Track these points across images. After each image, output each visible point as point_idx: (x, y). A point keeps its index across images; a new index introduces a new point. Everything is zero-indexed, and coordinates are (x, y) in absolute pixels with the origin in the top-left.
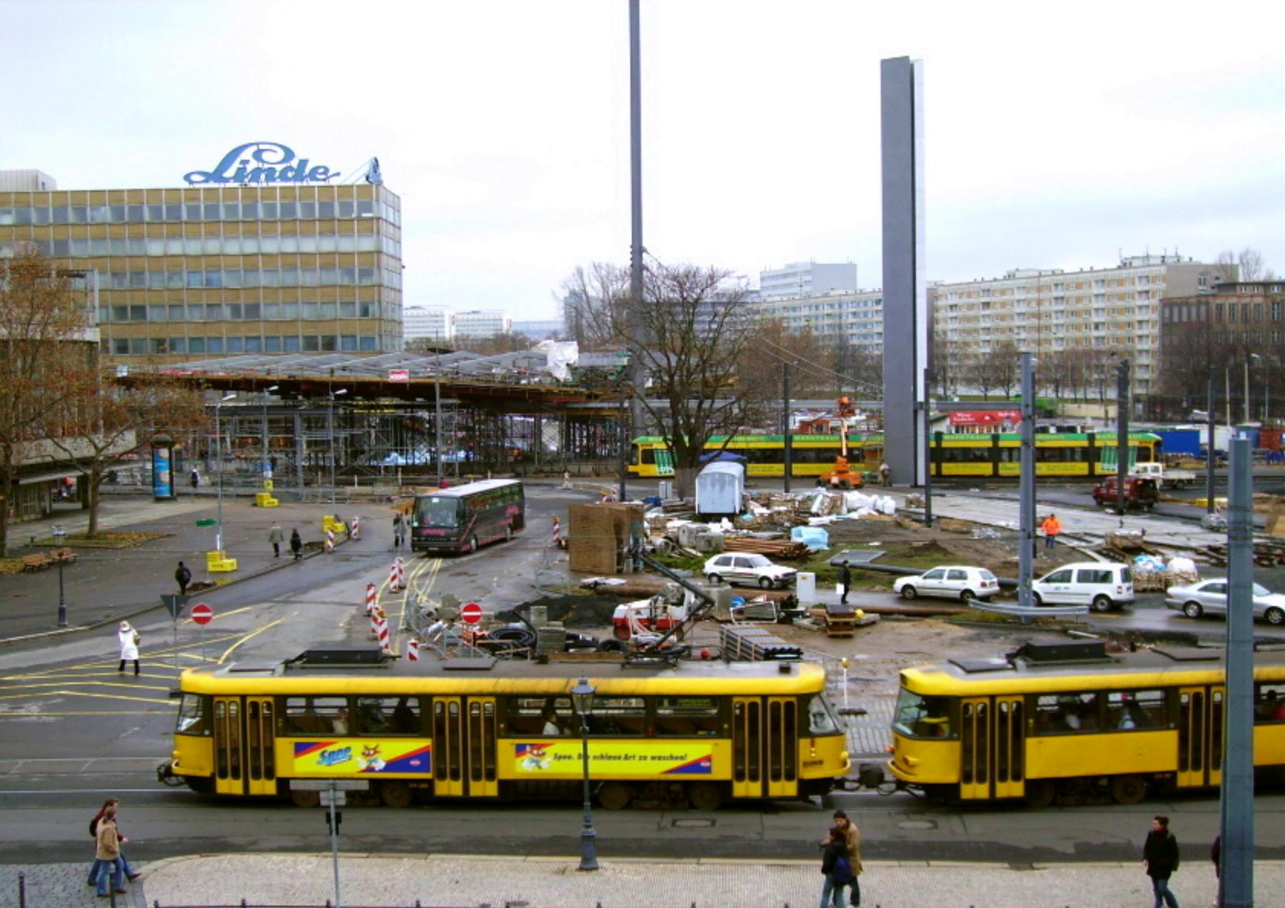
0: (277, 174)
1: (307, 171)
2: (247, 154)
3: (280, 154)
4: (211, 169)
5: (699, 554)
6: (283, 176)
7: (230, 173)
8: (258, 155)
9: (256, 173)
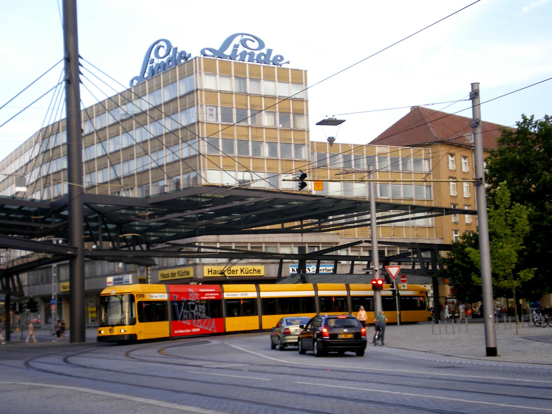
0: (255, 58)
1: (271, 59)
2: (237, 41)
3: (256, 45)
4: (217, 48)
5: (316, 344)
7: (228, 52)
8: (243, 43)
9: (243, 54)
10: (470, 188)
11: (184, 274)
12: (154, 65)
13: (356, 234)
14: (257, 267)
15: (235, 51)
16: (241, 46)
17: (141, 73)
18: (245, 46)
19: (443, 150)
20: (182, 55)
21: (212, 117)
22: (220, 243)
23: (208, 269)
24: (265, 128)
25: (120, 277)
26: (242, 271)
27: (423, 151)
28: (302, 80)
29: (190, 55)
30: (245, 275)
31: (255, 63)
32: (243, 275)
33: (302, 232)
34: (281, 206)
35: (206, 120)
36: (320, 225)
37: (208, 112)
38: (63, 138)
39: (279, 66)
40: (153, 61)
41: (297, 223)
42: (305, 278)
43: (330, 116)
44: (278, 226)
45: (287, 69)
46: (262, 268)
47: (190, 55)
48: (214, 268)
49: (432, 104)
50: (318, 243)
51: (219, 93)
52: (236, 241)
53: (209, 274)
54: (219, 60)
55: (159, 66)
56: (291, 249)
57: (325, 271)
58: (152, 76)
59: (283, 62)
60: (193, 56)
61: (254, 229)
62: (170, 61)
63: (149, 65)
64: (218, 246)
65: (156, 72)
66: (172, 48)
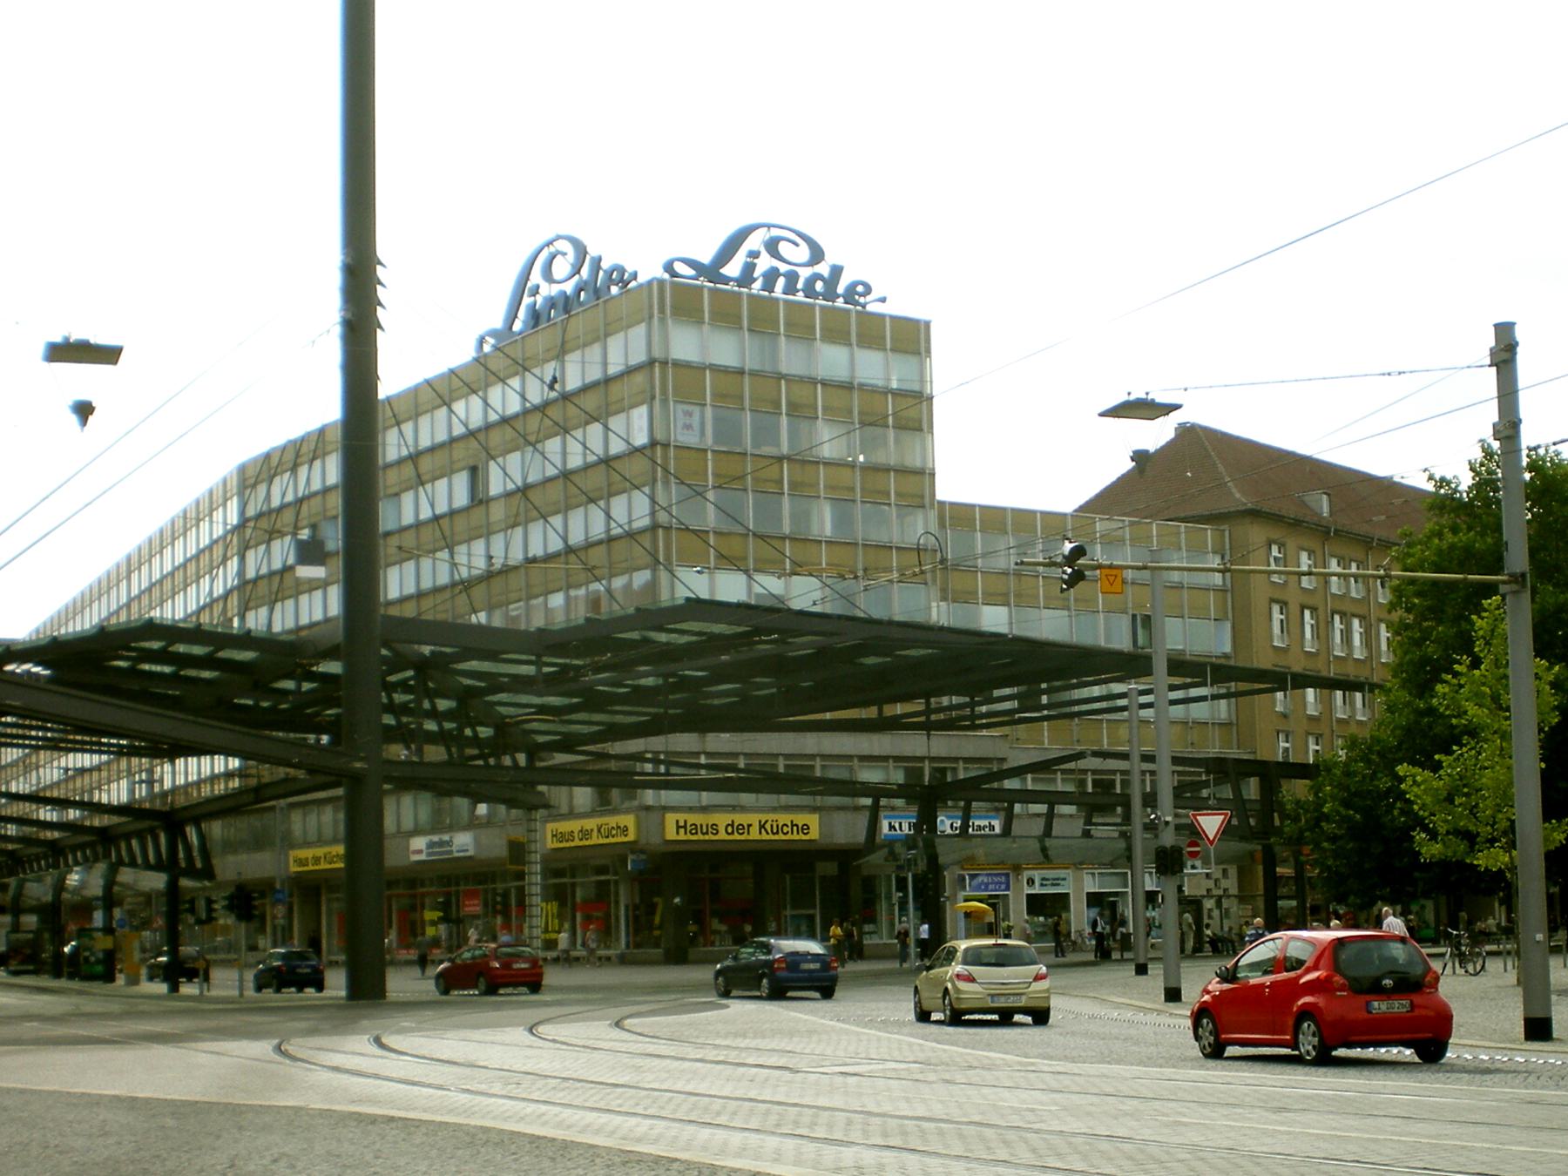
0: (800, 285)
1: (840, 290)
2: (755, 242)
3: (802, 253)
4: (706, 258)
6: (809, 290)
7: (733, 269)
8: (772, 246)
9: (771, 277)
10: (1318, 629)
11: (614, 832)
12: (539, 299)
13: (1045, 741)
14: (801, 819)
15: (749, 269)
16: (765, 255)
17: (506, 320)
18: (775, 254)
19: (1256, 534)
20: (614, 276)
21: (690, 432)
22: (709, 755)
23: (677, 822)
24: (825, 463)
25: (446, 837)
26: (762, 826)
27: (1209, 531)
28: (919, 342)
29: (634, 276)
30: (772, 837)
31: (800, 297)
32: (765, 836)
33: (928, 727)
34: (922, 652)
35: (675, 441)
36: (973, 711)
37: (680, 414)
38: (331, 470)
39: (859, 308)
40: (535, 291)
41: (918, 705)
42: (934, 847)
43: (1138, 394)
44: (871, 712)
45: (882, 317)
46: (813, 820)
47: (634, 276)
48: (693, 818)
49: (1400, 373)
50: (956, 760)
51: (708, 372)
52: (745, 751)
53: (678, 833)
54: (710, 289)
55: (552, 303)
56: (888, 774)
57: (987, 829)
58: (533, 327)
59: (869, 298)
60: (642, 279)
61: (791, 719)
62: (582, 290)
63: (527, 300)
64: (703, 760)
65: (544, 318)
66: (588, 257)
